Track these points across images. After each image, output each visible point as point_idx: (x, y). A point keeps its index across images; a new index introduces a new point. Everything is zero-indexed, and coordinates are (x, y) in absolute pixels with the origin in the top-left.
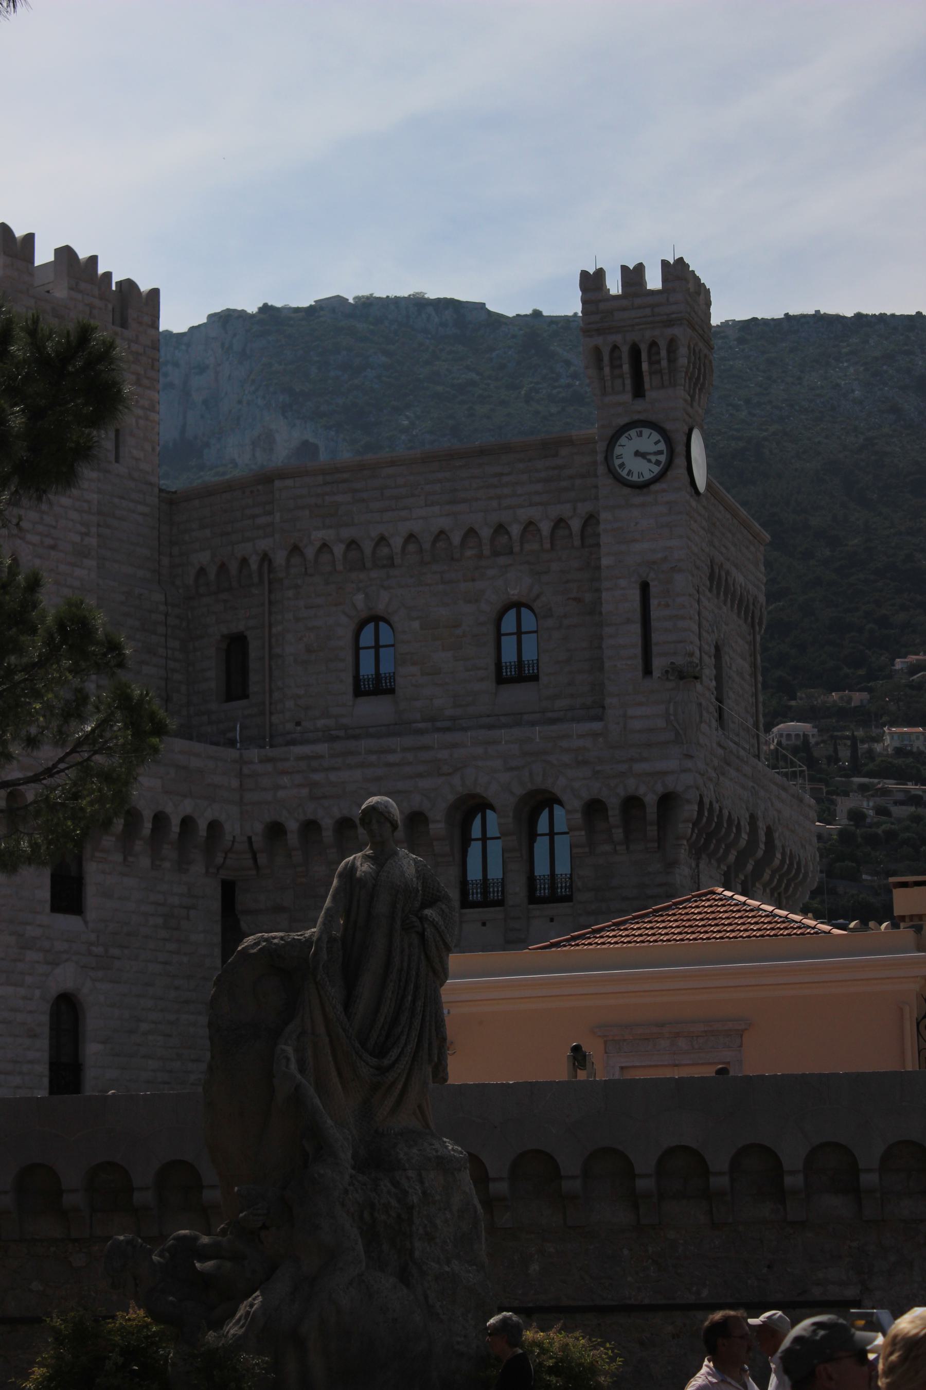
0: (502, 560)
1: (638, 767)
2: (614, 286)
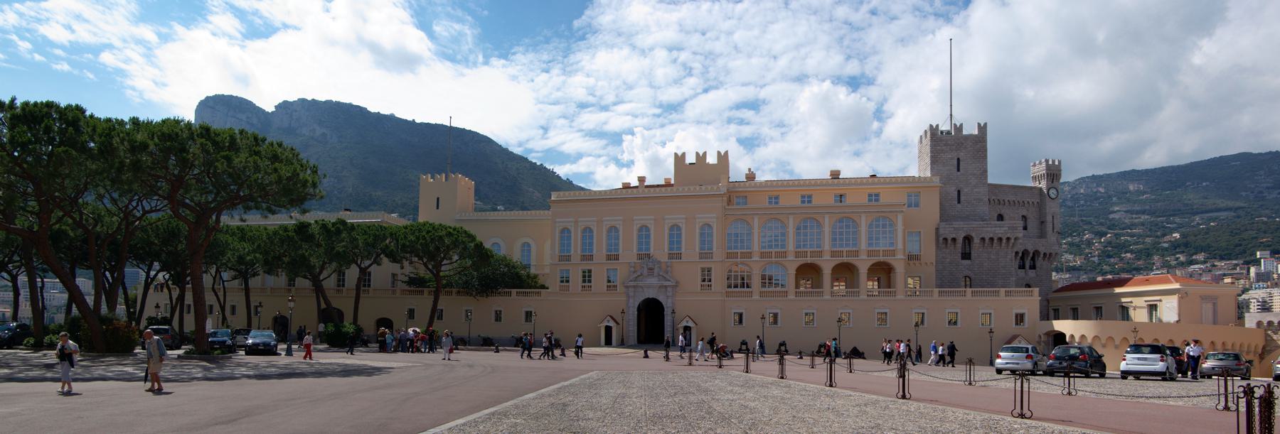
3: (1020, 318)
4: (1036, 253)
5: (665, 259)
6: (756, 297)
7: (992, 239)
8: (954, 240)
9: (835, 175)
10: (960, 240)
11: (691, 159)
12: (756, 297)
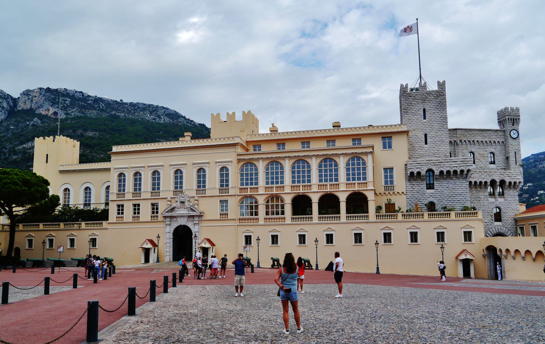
3: (468, 236)
4: (502, 183)
5: (194, 194)
6: (261, 222)
7: (448, 172)
8: (419, 173)
9: (337, 126)
11: (224, 118)
12: (261, 222)
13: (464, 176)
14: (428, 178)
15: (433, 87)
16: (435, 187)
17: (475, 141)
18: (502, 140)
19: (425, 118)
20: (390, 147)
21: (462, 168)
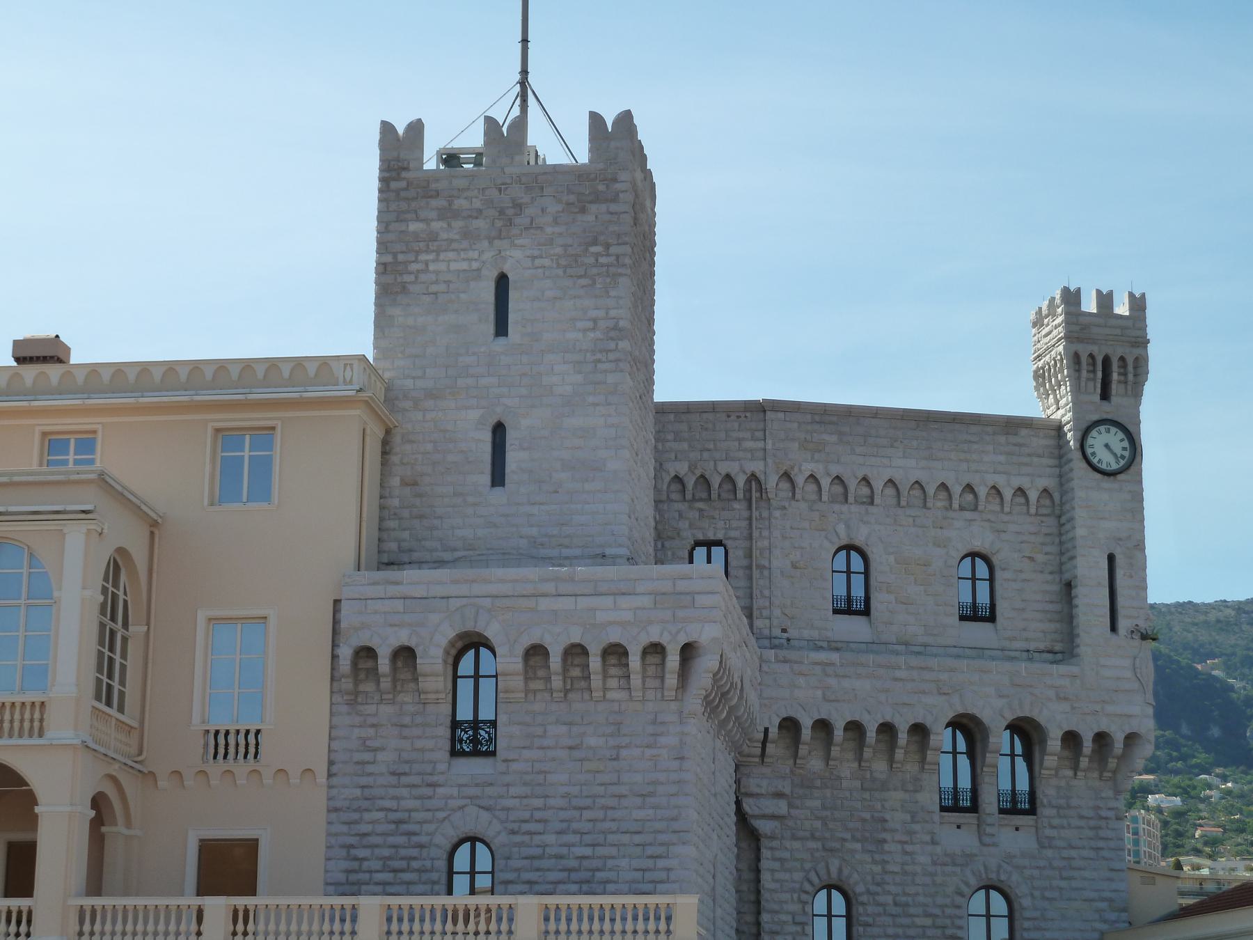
0: (968, 515)
1: (1110, 709)
2: (1090, 305)
7: (576, 652)
8: (405, 655)
10: (432, 659)
13: (672, 680)
14: (465, 687)
15: (560, 142)
16: (501, 744)
17: (878, 485)
18: (1043, 483)
19: (501, 328)
20: (261, 490)
21: (654, 634)
